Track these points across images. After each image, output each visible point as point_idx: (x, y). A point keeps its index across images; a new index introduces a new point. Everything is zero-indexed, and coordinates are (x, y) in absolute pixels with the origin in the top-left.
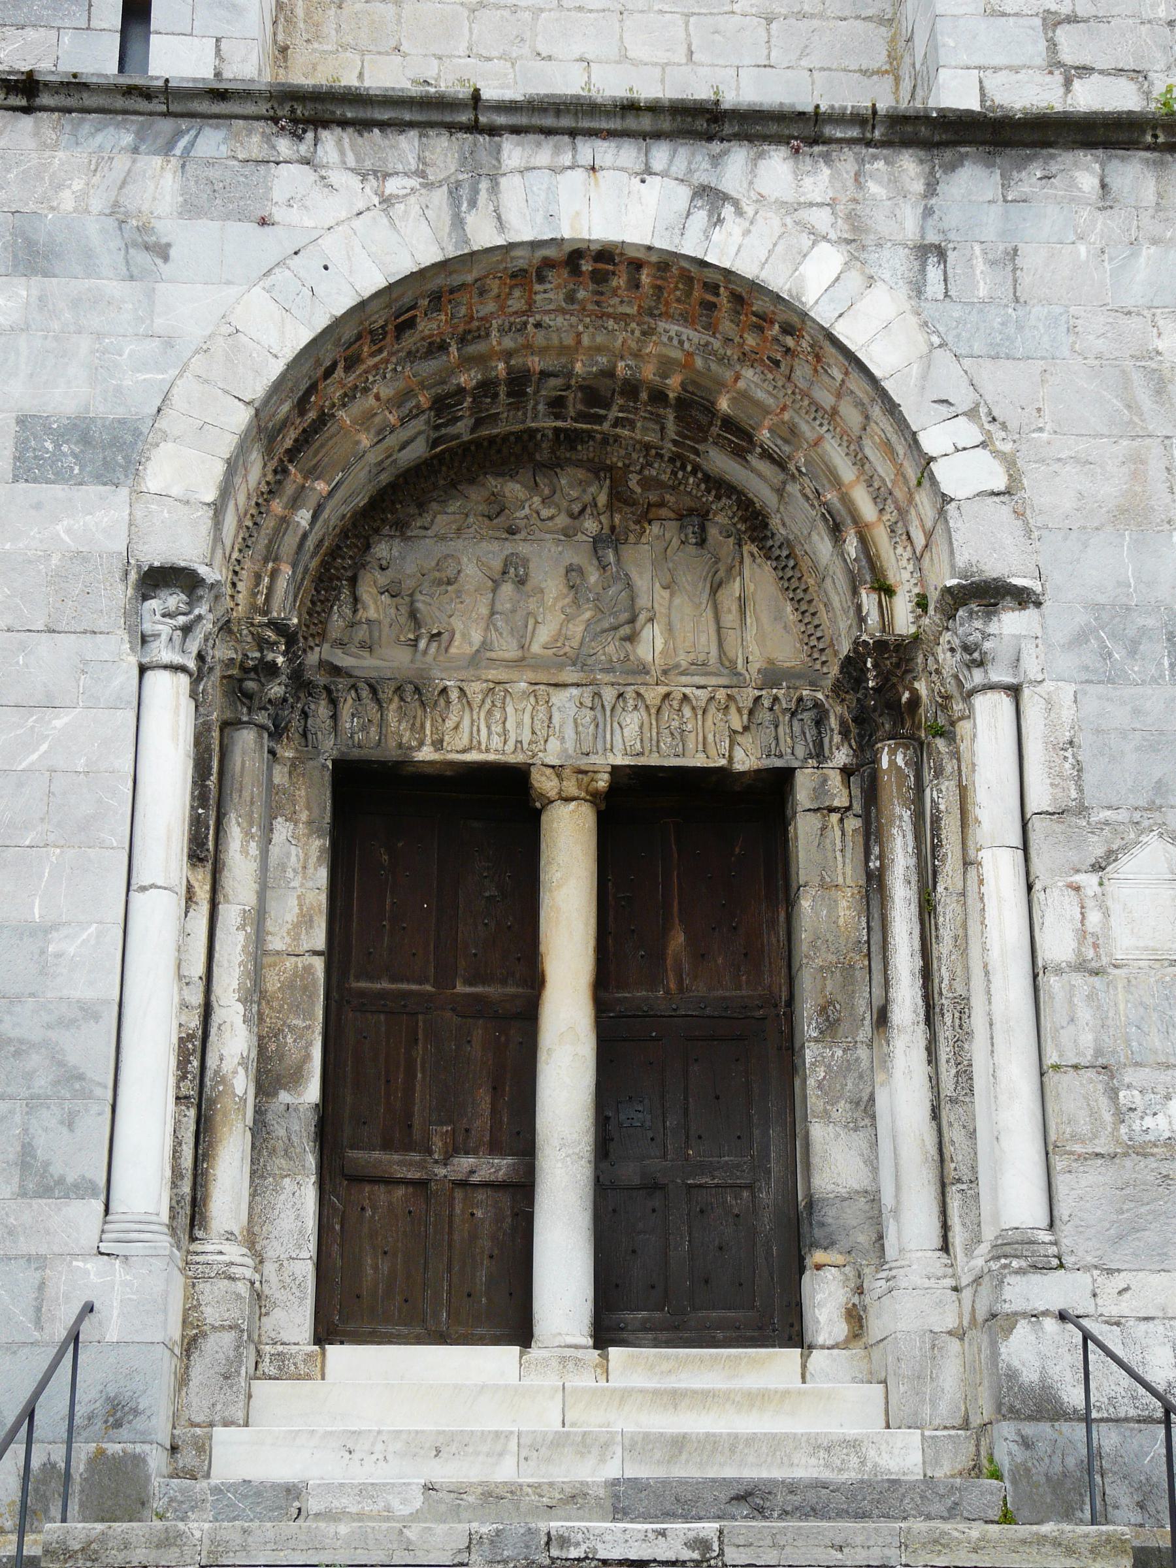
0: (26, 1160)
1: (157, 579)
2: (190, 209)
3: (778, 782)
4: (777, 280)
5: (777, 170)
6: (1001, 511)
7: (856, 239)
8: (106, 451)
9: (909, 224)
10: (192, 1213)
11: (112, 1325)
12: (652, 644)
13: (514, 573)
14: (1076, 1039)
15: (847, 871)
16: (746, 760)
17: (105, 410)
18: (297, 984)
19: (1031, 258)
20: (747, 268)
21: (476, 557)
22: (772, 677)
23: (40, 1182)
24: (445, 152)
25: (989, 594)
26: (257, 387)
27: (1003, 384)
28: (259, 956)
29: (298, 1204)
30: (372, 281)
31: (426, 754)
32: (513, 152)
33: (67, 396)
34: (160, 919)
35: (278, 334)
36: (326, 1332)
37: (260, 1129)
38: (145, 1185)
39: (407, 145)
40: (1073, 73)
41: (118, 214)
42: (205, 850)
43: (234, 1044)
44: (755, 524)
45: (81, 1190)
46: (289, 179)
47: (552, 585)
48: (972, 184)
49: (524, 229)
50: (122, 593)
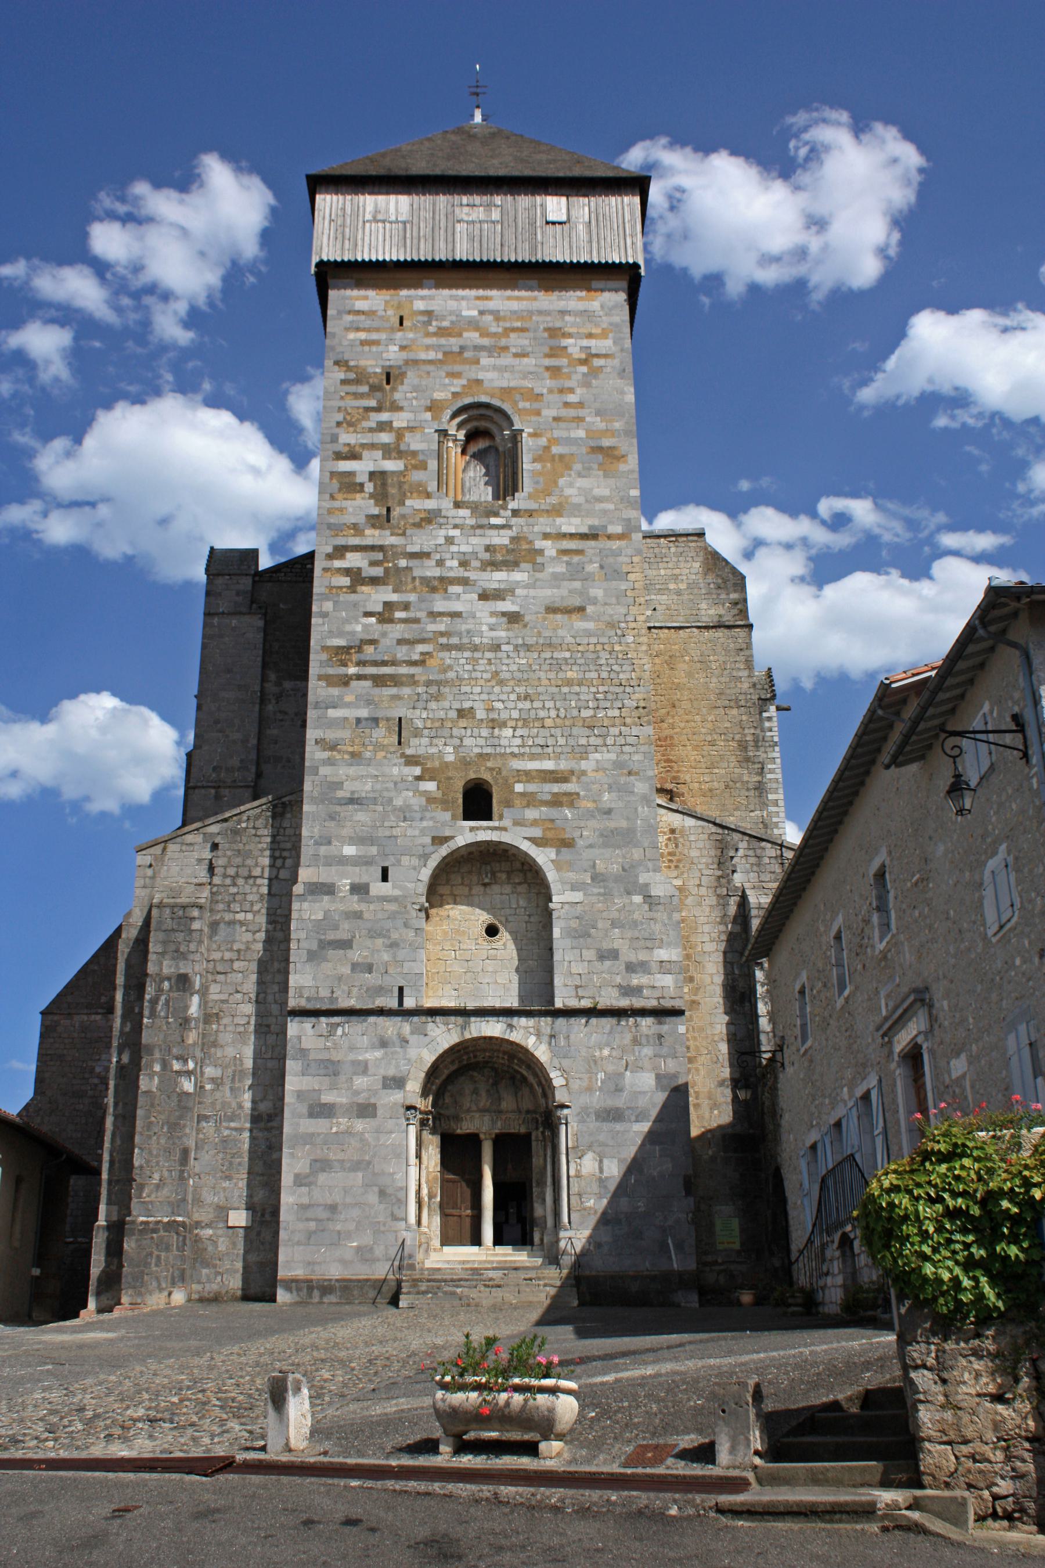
0: (392, 1214)
1: (409, 1108)
2: (412, 1033)
3: (528, 1136)
4: (523, 1043)
5: (523, 1021)
6: (565, 1089)
7: (538, 1035)
8: (399, 1083)
9: (548, 1031)
10: (419, 1223)
11: (408, 1242)
12: (504, 1105)
13: (476, 1092)
14: (574, 1189)
15: (541, 1153)
16: (523, 1130)
17: (399, 1075)
18: (435, 1178)
19: (572, 1037)
20: (517, 1041)
21: (468, 1088)
22: (528, 1112)
23: (395, 1218)
24: (460, 1020)
25: (563, 1106)
26: (426, 1069)
27: (566, 1063)
28: (428, 1173)
29: (437, 1220)
30: (446, 1046)
31: (459, 1131)
32: (473, 1019)
33: (391, 1072)
34: (413, 1171)
35: (429, 1058)
36: (442, 1244)
37: (429, 1206)
38: (412, 1219)
39: (453, 1019)
40: (581, 998)
41: (399, 1035)
42: (419, 1156)
43: (425, 1191)
44: (524, 1079)
45: (402, 1219)
46: (430, 1026)
47: (484, 1094)
48: (561, 1021)
49: (475, 1035)
50: (403, 1110)
